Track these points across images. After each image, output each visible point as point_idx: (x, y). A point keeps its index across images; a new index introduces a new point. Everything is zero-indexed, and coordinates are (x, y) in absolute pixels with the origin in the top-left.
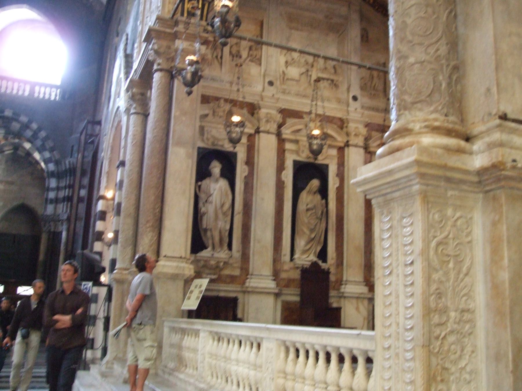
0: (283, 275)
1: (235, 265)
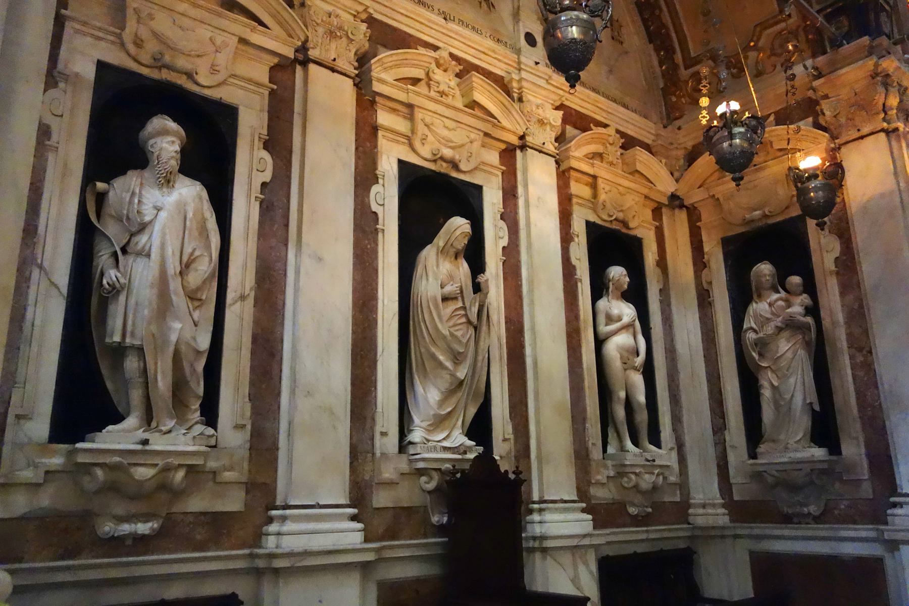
0: (381, 499)
1: (228, 475)
